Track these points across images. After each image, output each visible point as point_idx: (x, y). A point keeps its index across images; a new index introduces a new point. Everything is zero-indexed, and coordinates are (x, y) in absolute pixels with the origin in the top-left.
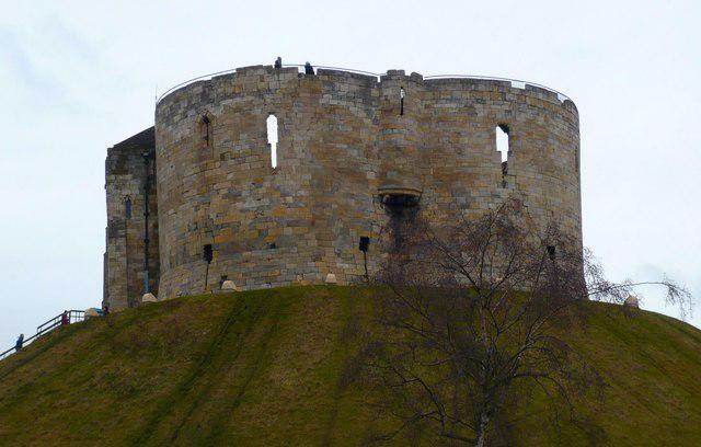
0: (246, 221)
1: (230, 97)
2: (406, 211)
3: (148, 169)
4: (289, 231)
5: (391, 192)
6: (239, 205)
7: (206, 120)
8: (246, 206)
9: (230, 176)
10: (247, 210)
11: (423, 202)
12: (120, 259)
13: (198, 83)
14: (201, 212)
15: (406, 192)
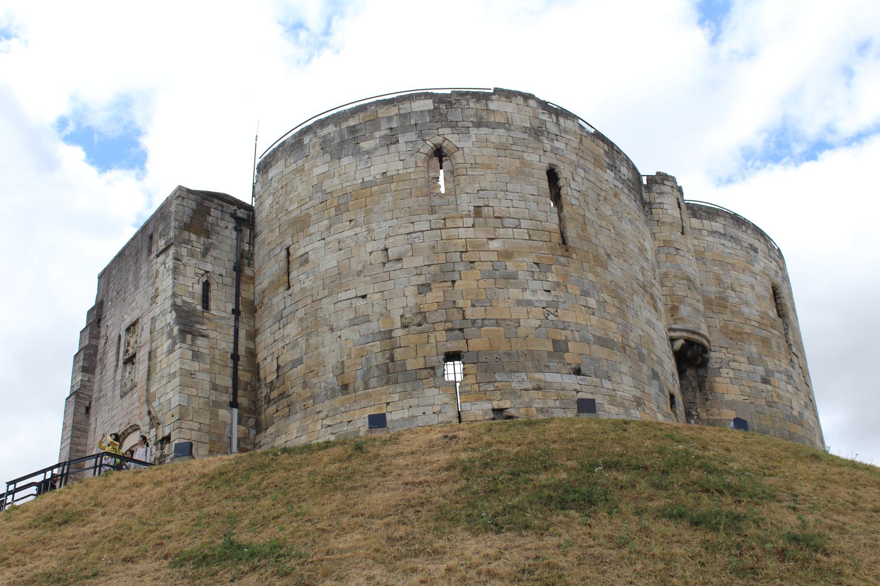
0: (530, 321)
1: (487, 125)
2: (690, 372)
3: (239, 240)
4: (599, 352)
5: (685, 334)
6: (515, 293)
7: (439, 153)
8: (528, 296)
9: (495, 245)
10: (529, 303)
11: (713, 364)
12: (200, 376)
13: (427, 95)
14: (435, 295)
15: (705, 342)
